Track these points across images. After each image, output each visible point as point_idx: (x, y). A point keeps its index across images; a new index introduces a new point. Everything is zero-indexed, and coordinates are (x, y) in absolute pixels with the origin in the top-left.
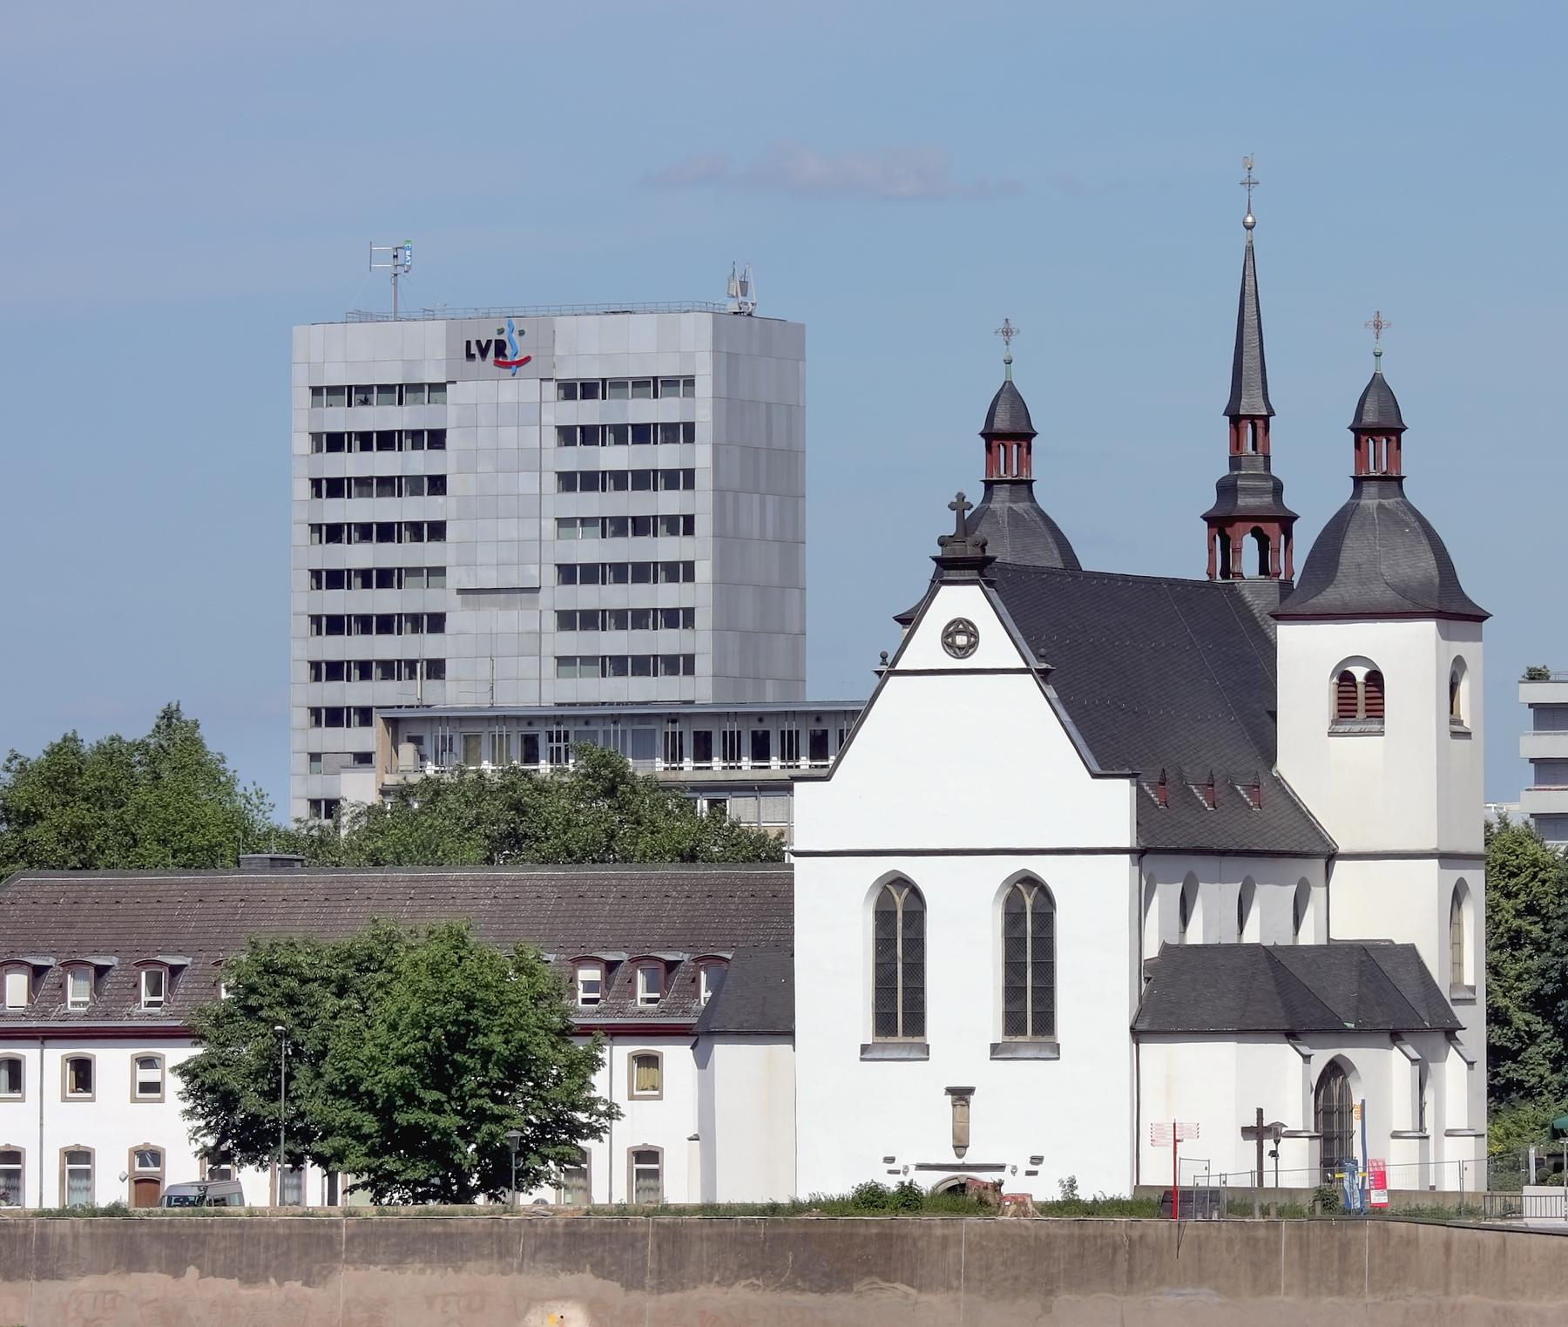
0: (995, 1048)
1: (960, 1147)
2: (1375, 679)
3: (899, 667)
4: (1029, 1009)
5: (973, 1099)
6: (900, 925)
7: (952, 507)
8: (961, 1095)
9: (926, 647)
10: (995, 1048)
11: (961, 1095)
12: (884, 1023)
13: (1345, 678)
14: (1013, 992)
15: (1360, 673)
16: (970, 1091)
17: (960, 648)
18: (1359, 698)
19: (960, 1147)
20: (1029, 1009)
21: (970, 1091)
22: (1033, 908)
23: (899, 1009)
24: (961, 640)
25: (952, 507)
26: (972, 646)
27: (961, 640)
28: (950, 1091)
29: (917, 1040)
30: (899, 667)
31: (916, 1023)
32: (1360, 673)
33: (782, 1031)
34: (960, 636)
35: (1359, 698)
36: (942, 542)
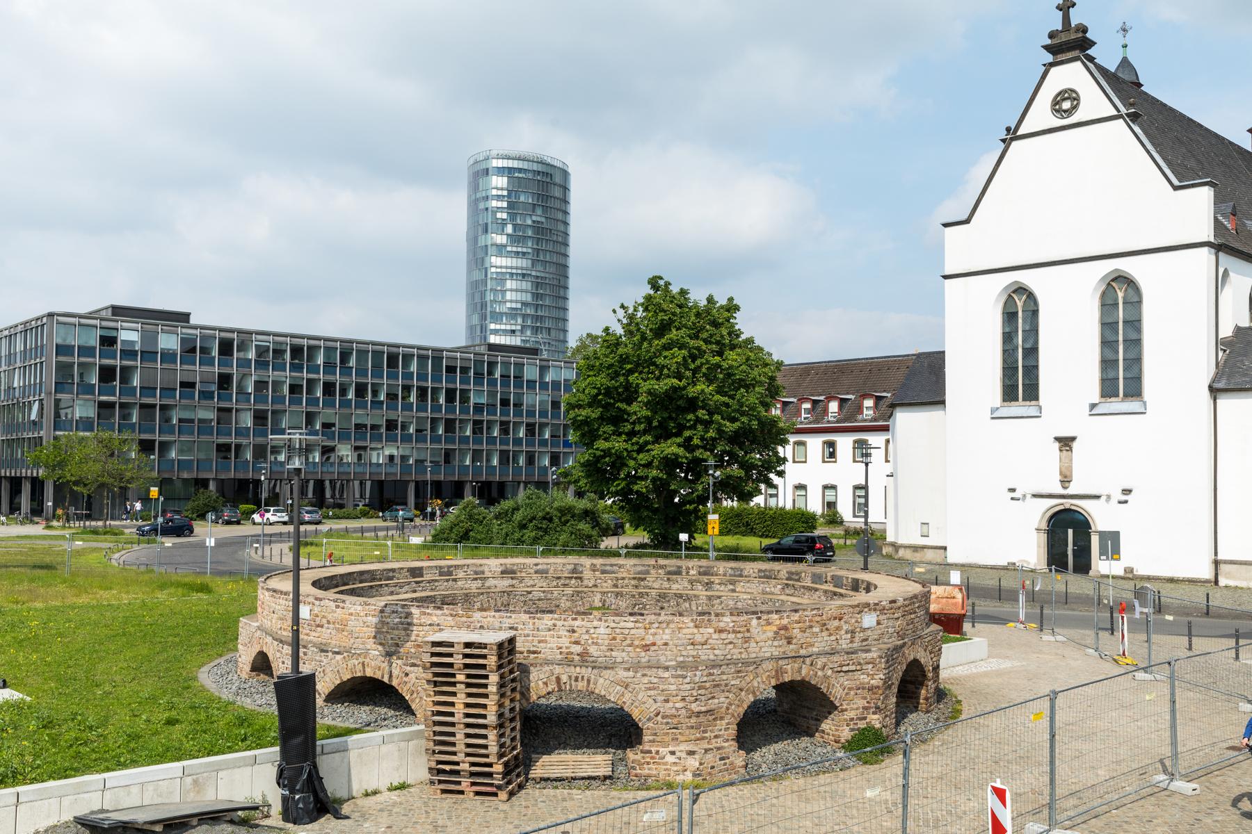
3: (1019, 133)
4: (1122, 375)
5: (1075, 445)
6: (1020, 321)
7: (1059, 8)
8: (1066, 443)
9: (1041, 115)
11: (1066, 443)
14: (1108, 364)
16: (1073, 439)
17: (1065, 111)
20: (1122, 375)
21: (1073, 439)
22: (1124, 298)
24: (1066, 105)
25: (1059, 8)
26: (1075, 108)
27: (1066, 105)
28: (1057, 439)
29: (1033, 403)
30: (1019, 133)
31: (1032, 393)
33: (937, 400)
34: (1066, 101)
36: (1052, 35)
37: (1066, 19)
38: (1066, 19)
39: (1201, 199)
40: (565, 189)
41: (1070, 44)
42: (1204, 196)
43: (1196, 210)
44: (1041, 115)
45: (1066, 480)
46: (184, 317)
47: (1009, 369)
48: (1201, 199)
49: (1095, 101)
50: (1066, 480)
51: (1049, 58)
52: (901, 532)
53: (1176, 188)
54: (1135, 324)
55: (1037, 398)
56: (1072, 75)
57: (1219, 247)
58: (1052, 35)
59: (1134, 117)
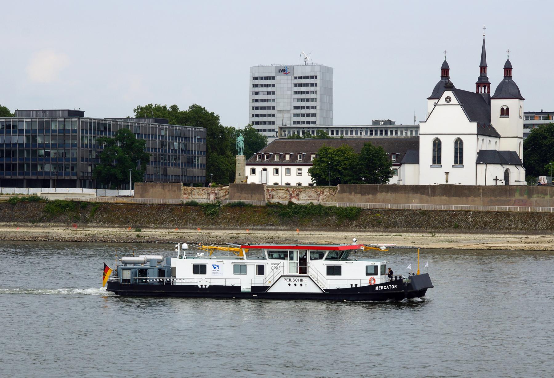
2: (508, 109)
11: (447, 173)
13: (503, 109)
14: (456, 157)
18: (505, 112)
23: (437, 160)
26: (450, 101)
27: (448, 100)
31: (439, 162)
35: (505, 112)
39: (475, 124)
45: (447, 181)
47: (434, 157)
48: (475, 124)
50: (447, 181)
54: (462, 149)
55: (440, 163)
57: (478, 134)
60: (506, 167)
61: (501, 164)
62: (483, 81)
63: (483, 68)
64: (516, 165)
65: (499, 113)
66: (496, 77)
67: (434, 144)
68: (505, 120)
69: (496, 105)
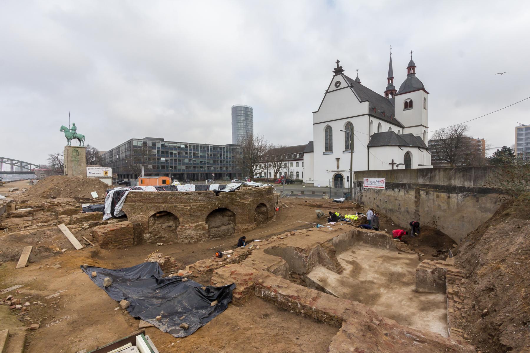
0: (343, 151)
1: (338, 167)
2: (411, 102)
10: (343, 151)
12: (327, 149)
13: (406, 103)
15: (408, 101)
18: (408, 105)
19: (338, 167)
24: (338, 85)
26: (340, 85)
27: (338, 85)
32: (408, 101)
34: (338, 84)
36: (335, 69)
37: (338, 65)
38: (338, 65)
40: (252, 113)
41: (339, 71)
42: (367, 103)
43: (365, 107)
44: (333, 87)
46: (163, 140)
49: (344, 84)
51: (334, 74)
52: (306, 179)
53: (361, 102)
56: (339, 78)
57: (370, 115)
58: (335, 69)
59: (352, 87)
60: (406, 150)
61: (400, 146)
62: (390, 88)
63: (391, 78)
64: (419, 148)
65: (403, 106)
66: (400, 78)
67: (326, 132)
68: (409, 112)
69: (400, 100)
